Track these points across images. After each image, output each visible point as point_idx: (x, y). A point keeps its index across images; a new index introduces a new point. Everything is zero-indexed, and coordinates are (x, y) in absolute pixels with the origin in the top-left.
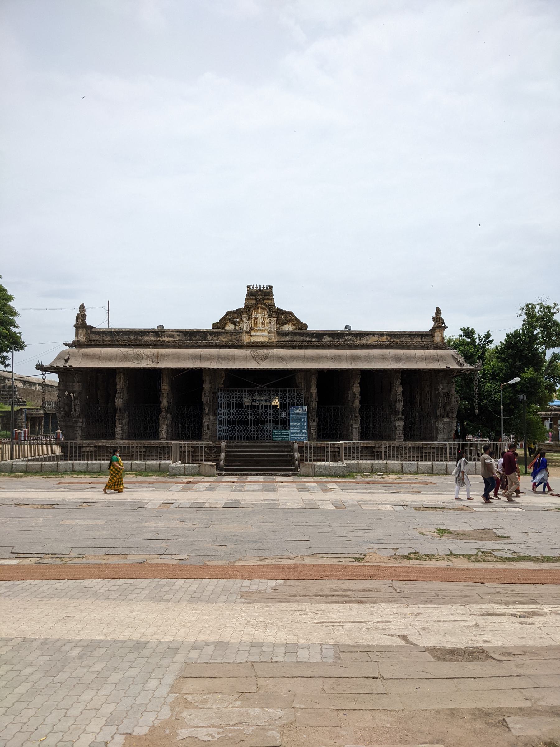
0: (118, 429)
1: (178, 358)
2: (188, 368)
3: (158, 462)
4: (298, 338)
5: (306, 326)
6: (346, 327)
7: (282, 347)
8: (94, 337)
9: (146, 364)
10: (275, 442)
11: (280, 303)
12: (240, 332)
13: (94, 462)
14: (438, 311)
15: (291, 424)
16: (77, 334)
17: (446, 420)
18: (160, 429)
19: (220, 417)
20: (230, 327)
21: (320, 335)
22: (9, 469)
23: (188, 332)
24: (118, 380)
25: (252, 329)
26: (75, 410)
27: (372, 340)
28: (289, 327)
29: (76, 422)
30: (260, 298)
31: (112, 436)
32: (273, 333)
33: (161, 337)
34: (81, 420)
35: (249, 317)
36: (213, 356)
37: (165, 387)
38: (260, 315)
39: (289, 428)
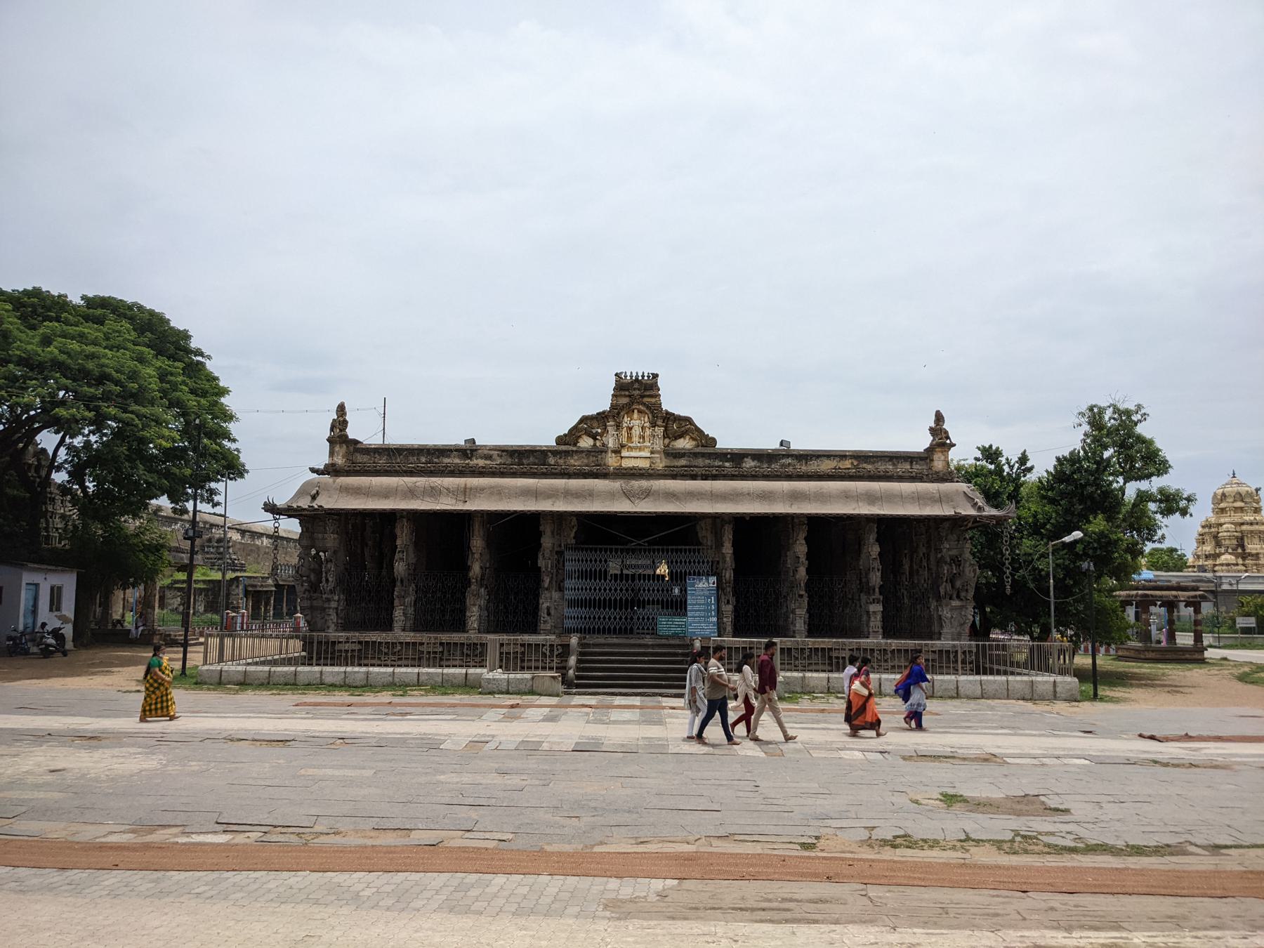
0: (398, 614)
1: (499, 493)
2: (515, 512)
3: (464, 671)
4: (700, 462)
5: (714, 441)
6: (781, 444)
7: (674, 477)
8: (360, 458)
9: (446, 504)
10: (661, 637)
11: (670, 404)
12: (603, 450)
13: (356, 669)
14: (939, 418)
15: (689, 608)
16: (332, 454)
17: (956, 603)
18: (468, 614)
19: (569, 595)
20: (586, 442)
21: (737, 457)
22: (217, 680)
23: (516, 451)
24: (398, 531)
25: (623, 446)
26: (327, 580)
27: (827, 466)
28: (684, 444)
29: (328, 600)
30: (636, 393)
31: (388, 625)
32: (658, 452)
33: (470, 459)
34: (336, 598)
35: (618, 426)
36: (557, 490)
37: (477, 543)
38: (636, 422)
39: (685, 615)
